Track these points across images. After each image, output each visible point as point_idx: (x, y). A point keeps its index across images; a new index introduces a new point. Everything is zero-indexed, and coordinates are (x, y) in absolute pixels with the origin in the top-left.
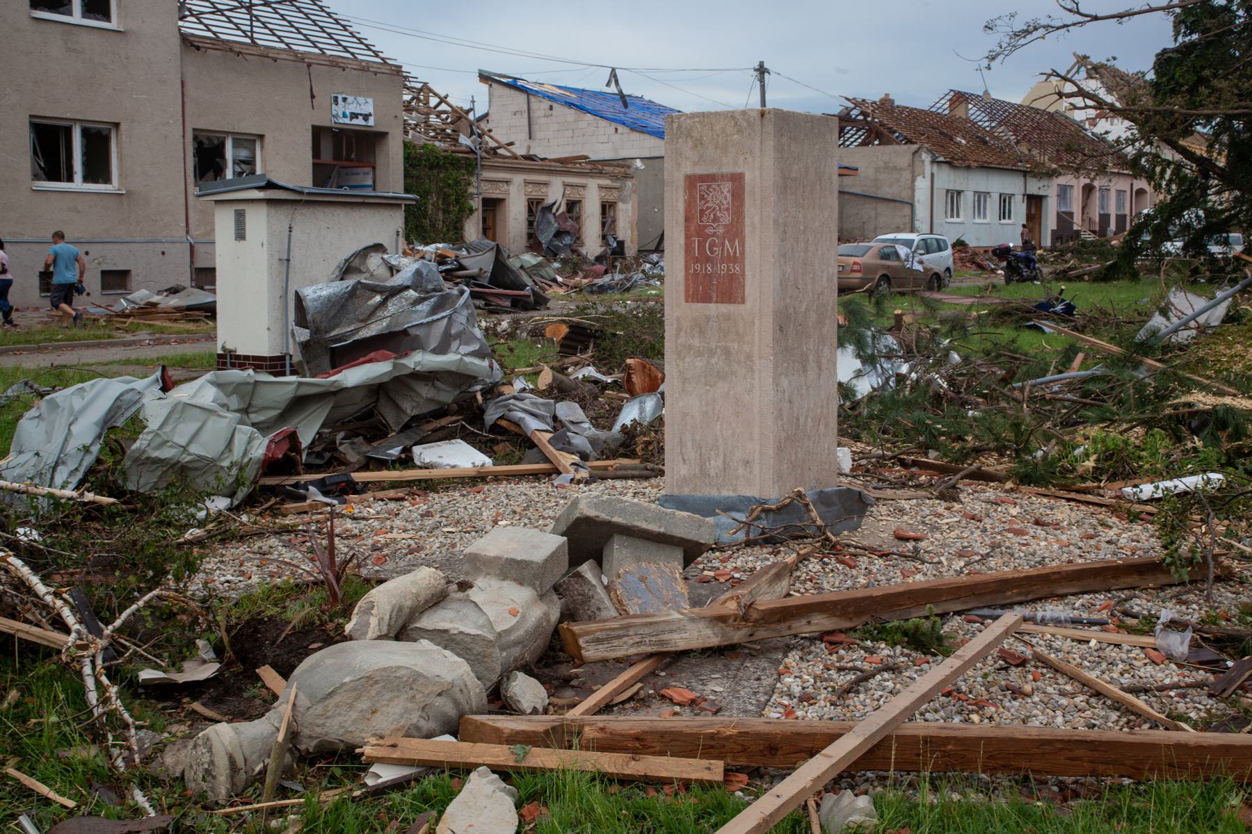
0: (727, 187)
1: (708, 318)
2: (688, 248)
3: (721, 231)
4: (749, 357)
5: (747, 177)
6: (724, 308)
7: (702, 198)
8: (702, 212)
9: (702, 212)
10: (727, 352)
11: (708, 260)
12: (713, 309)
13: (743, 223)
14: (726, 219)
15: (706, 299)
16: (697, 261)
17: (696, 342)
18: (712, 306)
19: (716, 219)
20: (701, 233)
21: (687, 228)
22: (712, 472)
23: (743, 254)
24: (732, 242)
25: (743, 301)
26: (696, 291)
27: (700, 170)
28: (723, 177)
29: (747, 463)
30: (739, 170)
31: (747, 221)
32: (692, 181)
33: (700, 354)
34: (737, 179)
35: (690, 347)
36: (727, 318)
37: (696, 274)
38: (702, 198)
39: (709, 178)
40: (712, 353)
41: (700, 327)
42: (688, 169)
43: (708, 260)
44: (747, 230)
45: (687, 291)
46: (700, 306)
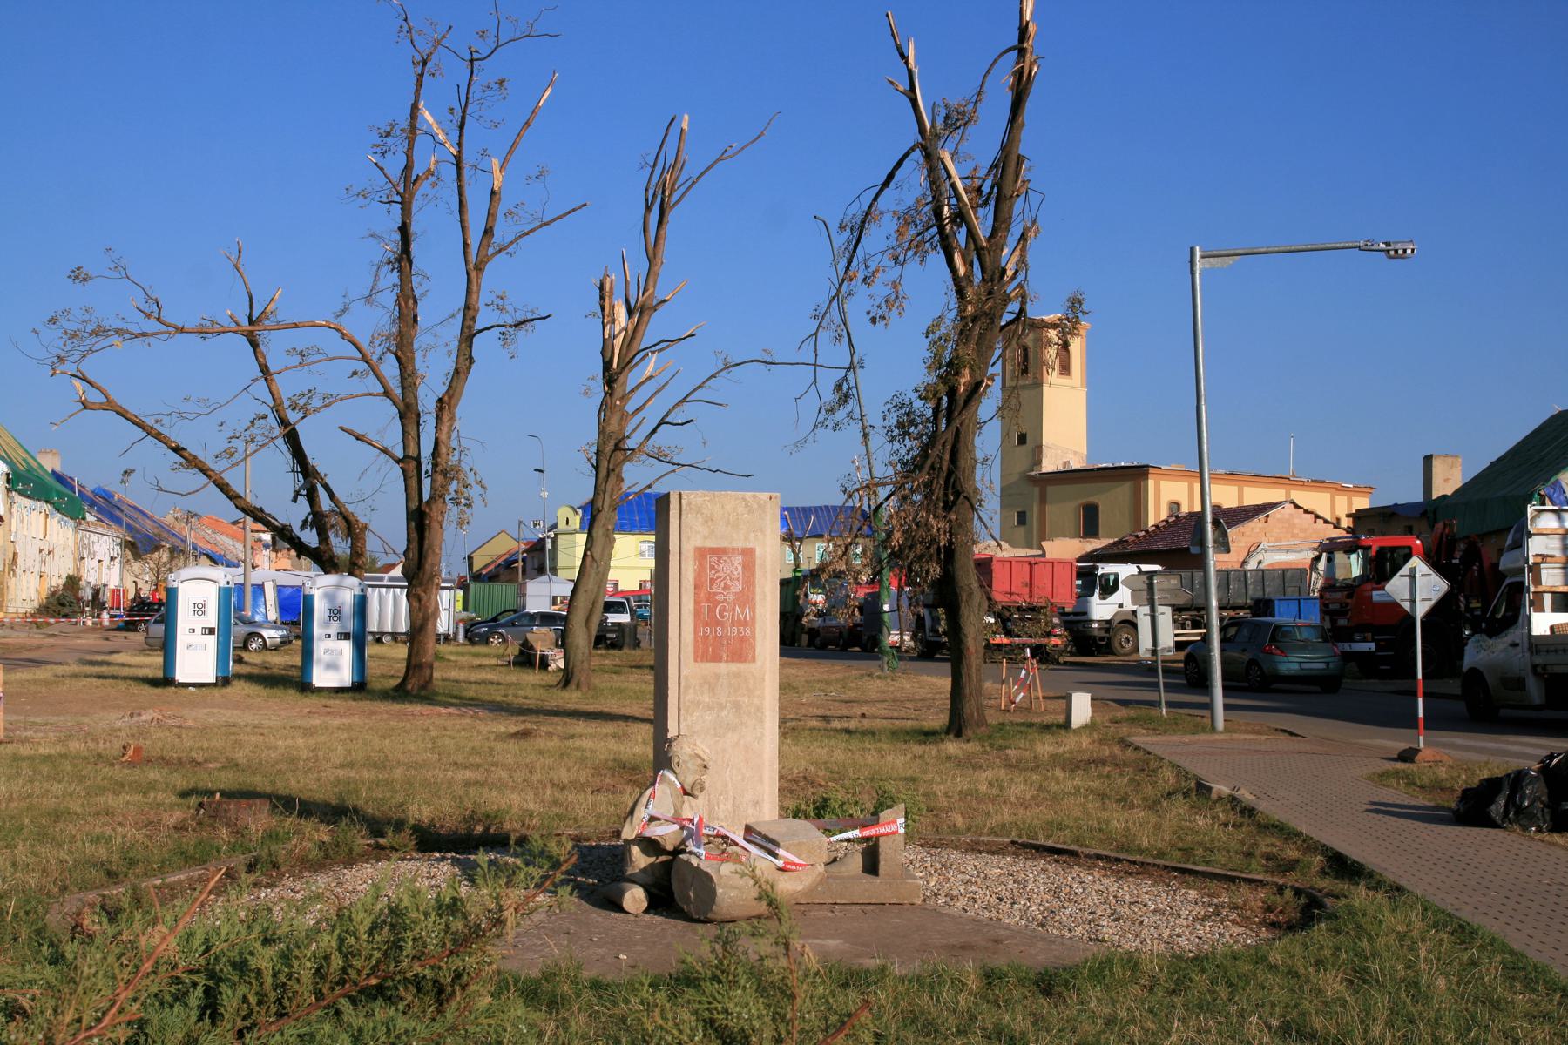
0: (737, 560)
1: (718, 676)
2: (697, 613)
3: (731, 598)
4: (759, 709)
5: (758, 552)
6: (734, 667)
7: (712, 568)
8: (712, 581)
9: (712, 581)
10: (737, 706)
11: (718, 623)
12: (723, 667)
13: (753, 592)
14: (737, 587)
15: (716, 658)
16: (707, 624)
17: (706, 699)
18: (722, 665)
19: (726, 587)
20: (711, 599)
21: (696, 595)
22: (721, 815)
23: (753, 618)
24: (742, 608)
25: (754, 659)
26: (705, 652)
27: (709, 544)
28: (734, 550)
29: (756, 803)
30: (749, 545)
31: (758, 590)
32: (702, 553)
33: (709, 708)
34: (748, 553)
35: (699, 703)
36: (737, 675)
37: (705, 637)
38: (712, 568)
39: (723, 551)
40: (722, 707)
41: (710, 684)
42: (699, 543)
43: (718, 623)
44: (758, 598)
45: (696, 652)
46: (710, 665)
